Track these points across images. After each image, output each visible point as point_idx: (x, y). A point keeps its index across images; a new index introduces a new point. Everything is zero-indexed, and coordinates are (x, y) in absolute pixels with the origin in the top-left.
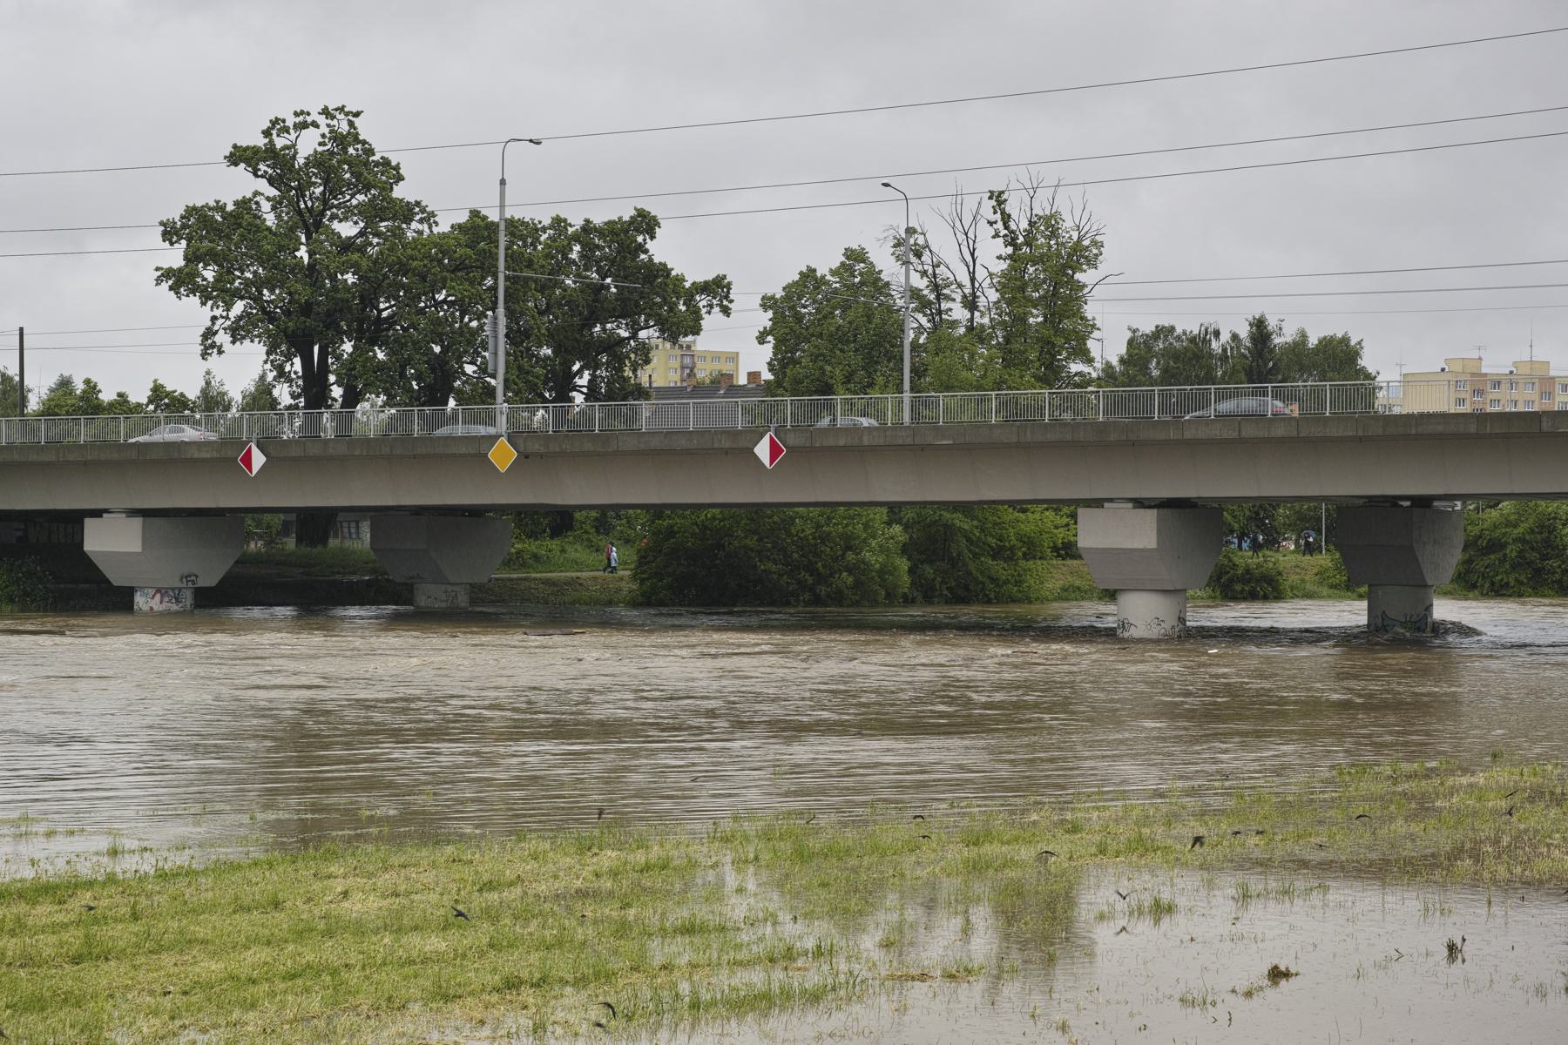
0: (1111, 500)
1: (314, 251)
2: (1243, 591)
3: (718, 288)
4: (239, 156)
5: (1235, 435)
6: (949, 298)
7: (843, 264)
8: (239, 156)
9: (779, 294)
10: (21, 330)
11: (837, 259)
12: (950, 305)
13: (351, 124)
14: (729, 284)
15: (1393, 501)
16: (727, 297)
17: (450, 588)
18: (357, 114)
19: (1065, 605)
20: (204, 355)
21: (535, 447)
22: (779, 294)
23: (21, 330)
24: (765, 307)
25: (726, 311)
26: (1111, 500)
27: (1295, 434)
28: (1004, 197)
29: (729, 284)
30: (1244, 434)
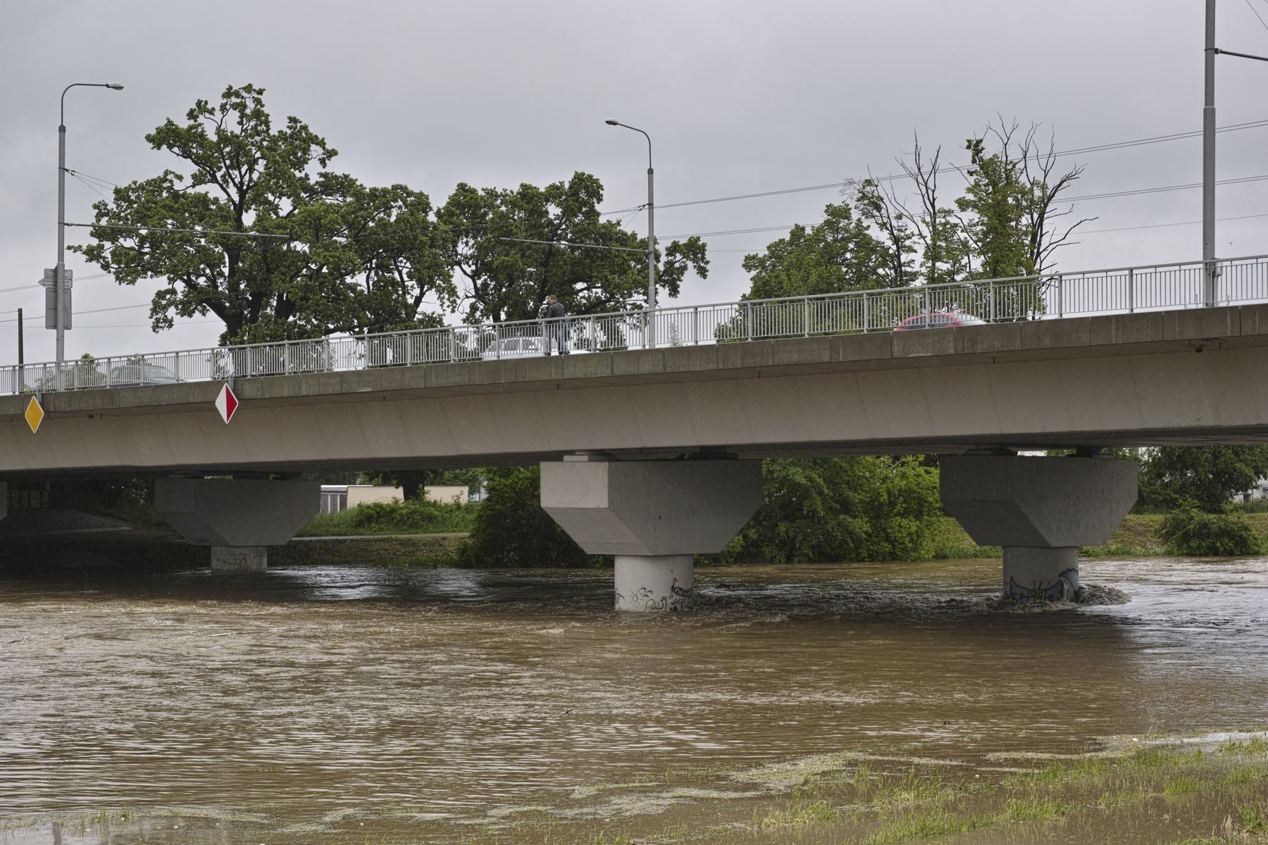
0: (572, 453)
1: (253, 226)
2: (1199, 547)
3: (694, 249)
4: (166, 137)
5: (607, 372)
6: (911, 250)
7: (827, 222)
8: (166, 137)
9: (763, 252)
10: (20, 311)
11: (820, 218)
12: (912, 256)
13: (258, 101)
14: (704, 245)
15: (1003, 446)
16: (703, 258)
17: (238, 551)
18: (260, 92)
19: (838, 568)
20: (155, 328)
21: (62, 406)
22: (763, 252)
23: (20, 311)
24: (748, 267)
25: (703, 272)
26: (572, 453)
27: (661, 369)
28: (982, 145)
29: (704, 245)
30: (616, 372)
